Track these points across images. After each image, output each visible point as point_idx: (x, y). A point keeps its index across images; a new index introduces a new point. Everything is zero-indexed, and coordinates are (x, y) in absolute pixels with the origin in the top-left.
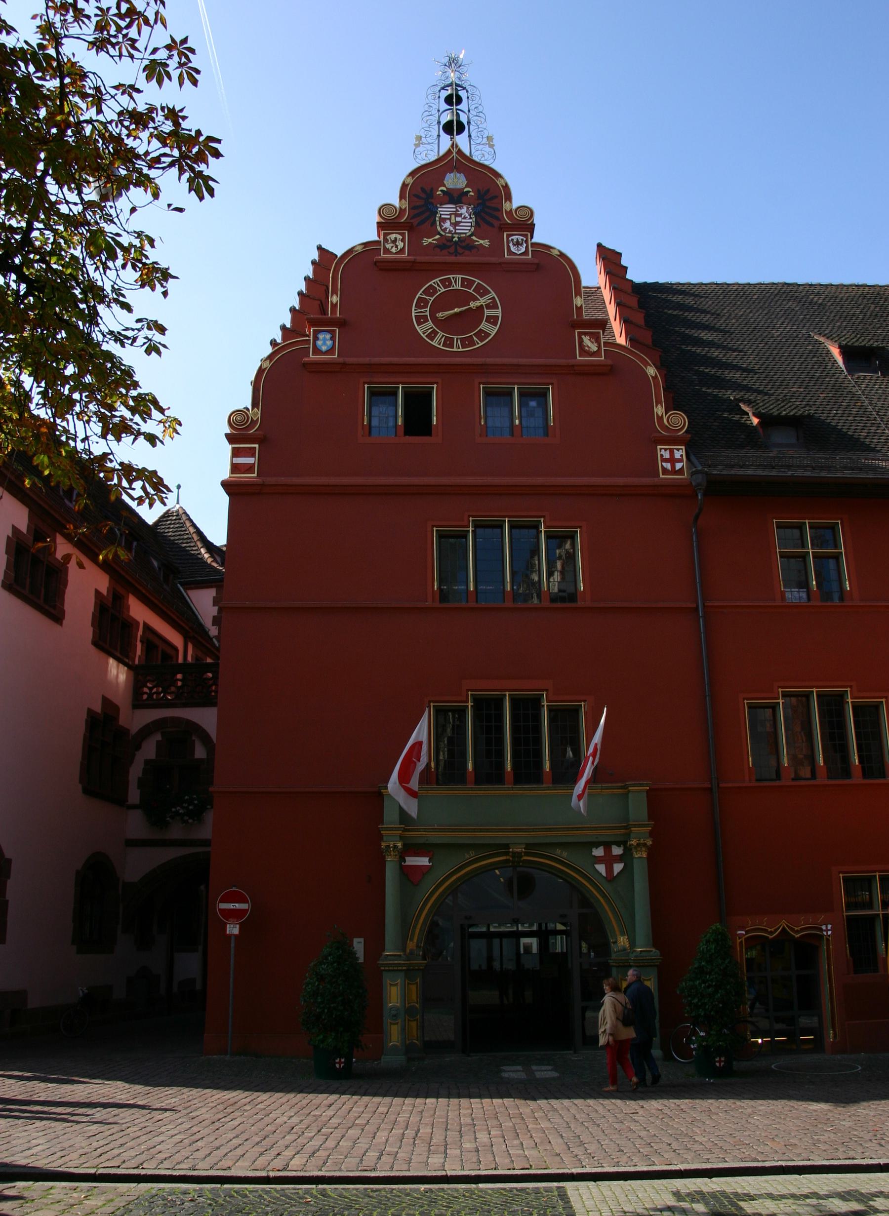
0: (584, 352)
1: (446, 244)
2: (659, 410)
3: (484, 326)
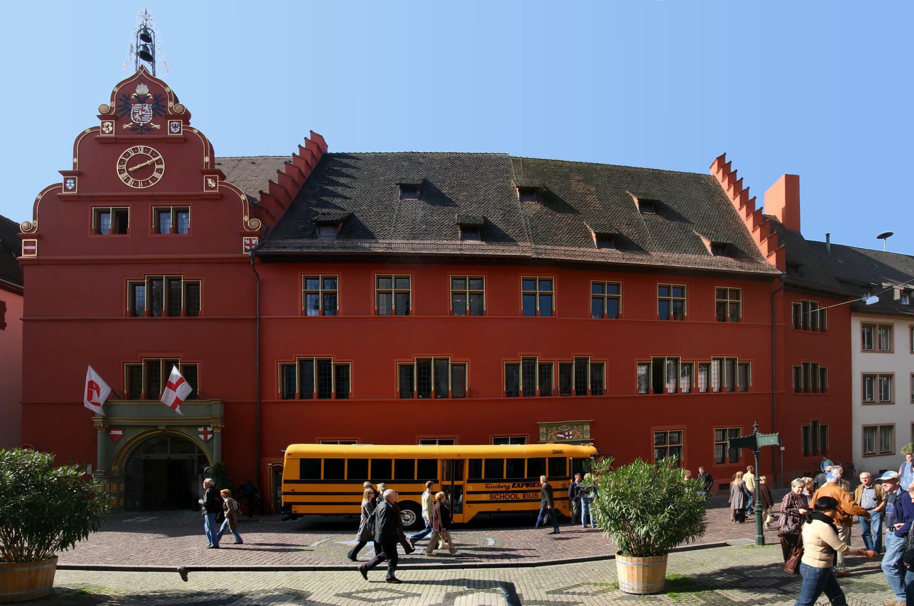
0: (208, 187)
1: (136, 128)
2: (246, 218)
3: (155, 174)
